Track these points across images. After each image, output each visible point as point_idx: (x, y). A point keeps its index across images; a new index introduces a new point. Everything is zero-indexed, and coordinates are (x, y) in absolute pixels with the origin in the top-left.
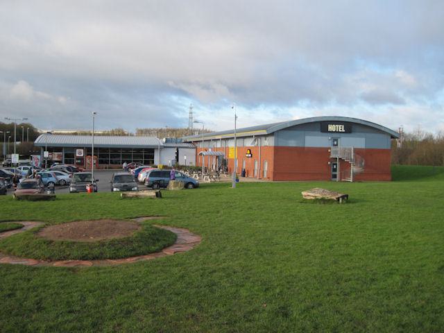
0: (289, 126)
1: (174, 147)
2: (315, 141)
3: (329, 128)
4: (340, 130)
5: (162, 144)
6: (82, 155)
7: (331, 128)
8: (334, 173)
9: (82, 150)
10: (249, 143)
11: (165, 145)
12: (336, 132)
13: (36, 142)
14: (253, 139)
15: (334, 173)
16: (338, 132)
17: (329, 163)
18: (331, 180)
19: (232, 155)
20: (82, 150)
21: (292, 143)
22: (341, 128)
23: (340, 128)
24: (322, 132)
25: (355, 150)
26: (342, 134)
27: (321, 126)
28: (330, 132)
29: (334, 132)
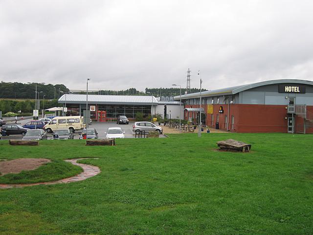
0: (251, 88)
1: (163, 104)
2: (274, 100)
3: (286, 89)
4: (295, 91)
5: (157, 102)
6: (95, 110)
7: (287, 89)
8: (290, 126)
9: (94, 107)
10: (218, 101)
11: (159, 103)
12: (291, 92)
13: (59, 100)
14: (224, 98)
15: (290, 126)
16: (294, 92)
17: (286, 118)
18: (287, 133)
19: (210, 110)
20: (94, 107)
21: (254, 102)
22: (296, 89)
23: (295, 89)
24: (279, 92)
25: (307, 106)
26: (297, 94)
27: (279, 87)
28: (287, 92)
29: (290, 92)
